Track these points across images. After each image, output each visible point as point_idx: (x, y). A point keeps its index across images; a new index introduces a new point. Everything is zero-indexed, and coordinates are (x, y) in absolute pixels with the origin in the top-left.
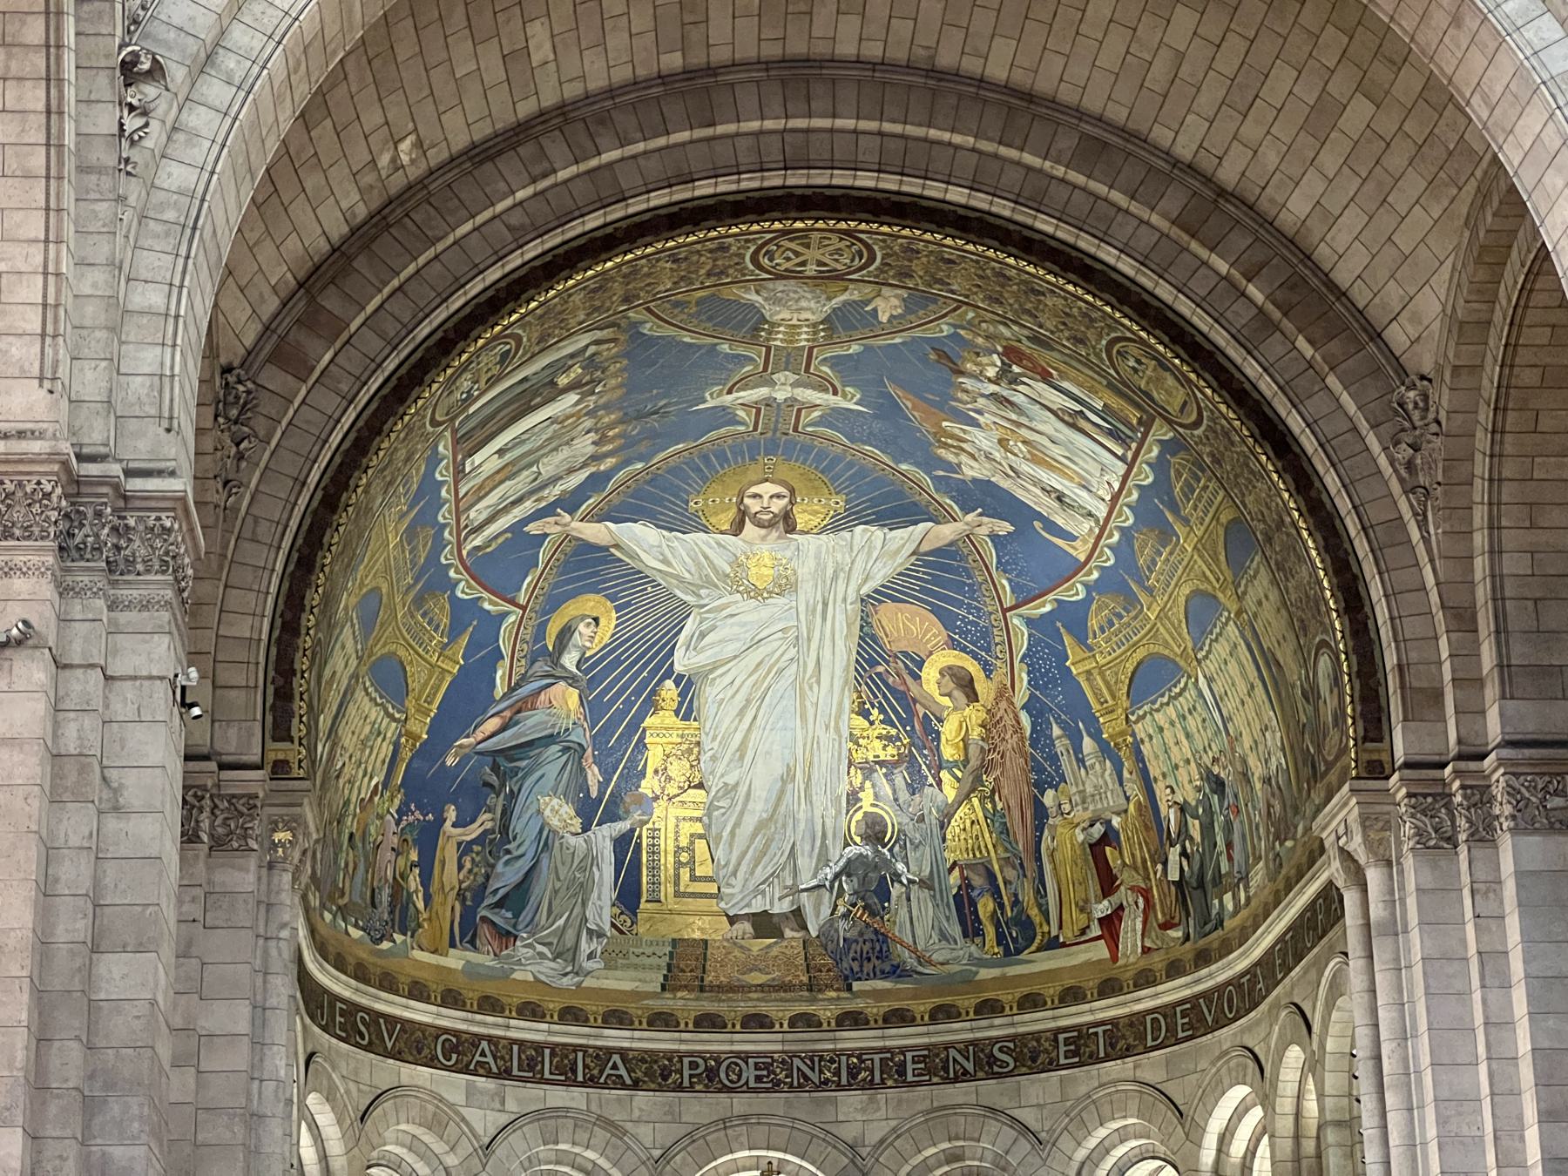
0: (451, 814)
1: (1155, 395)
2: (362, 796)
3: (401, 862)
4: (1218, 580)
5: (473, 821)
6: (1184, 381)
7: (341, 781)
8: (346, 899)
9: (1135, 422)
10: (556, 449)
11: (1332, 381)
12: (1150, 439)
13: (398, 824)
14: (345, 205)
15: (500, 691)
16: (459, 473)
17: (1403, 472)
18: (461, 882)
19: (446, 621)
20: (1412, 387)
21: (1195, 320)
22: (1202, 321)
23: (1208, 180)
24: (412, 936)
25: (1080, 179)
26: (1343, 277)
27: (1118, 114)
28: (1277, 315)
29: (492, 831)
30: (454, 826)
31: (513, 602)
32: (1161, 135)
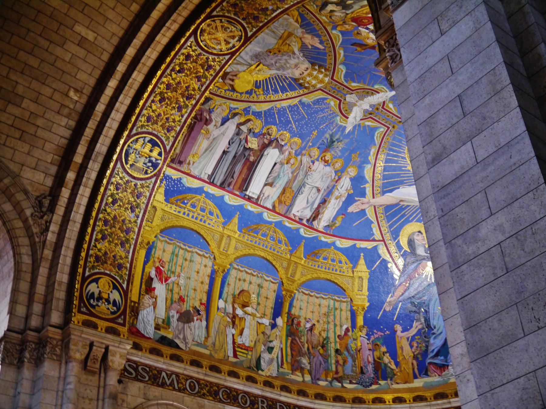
0: (398, 328)
2: (338, 333)
3: (377, 354)
5: (411, 327)
7: (316, 332)
8: (341, 374)
10: (306, 175)
13: (368, 339)
14: (63, 124)
15: (397, 274)
16: (249, 199)
18: (413, 353)
19: (344, 258)
24: (391, 380)
29: (423, 328)
30: (402, 332)
31: (374, 240)
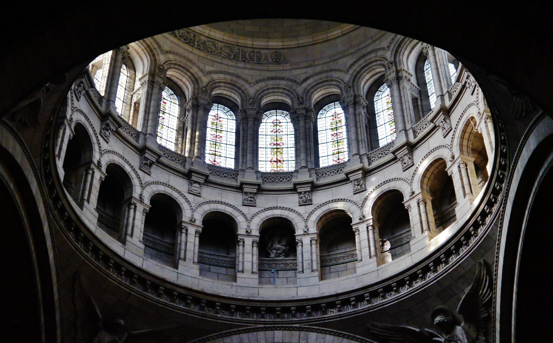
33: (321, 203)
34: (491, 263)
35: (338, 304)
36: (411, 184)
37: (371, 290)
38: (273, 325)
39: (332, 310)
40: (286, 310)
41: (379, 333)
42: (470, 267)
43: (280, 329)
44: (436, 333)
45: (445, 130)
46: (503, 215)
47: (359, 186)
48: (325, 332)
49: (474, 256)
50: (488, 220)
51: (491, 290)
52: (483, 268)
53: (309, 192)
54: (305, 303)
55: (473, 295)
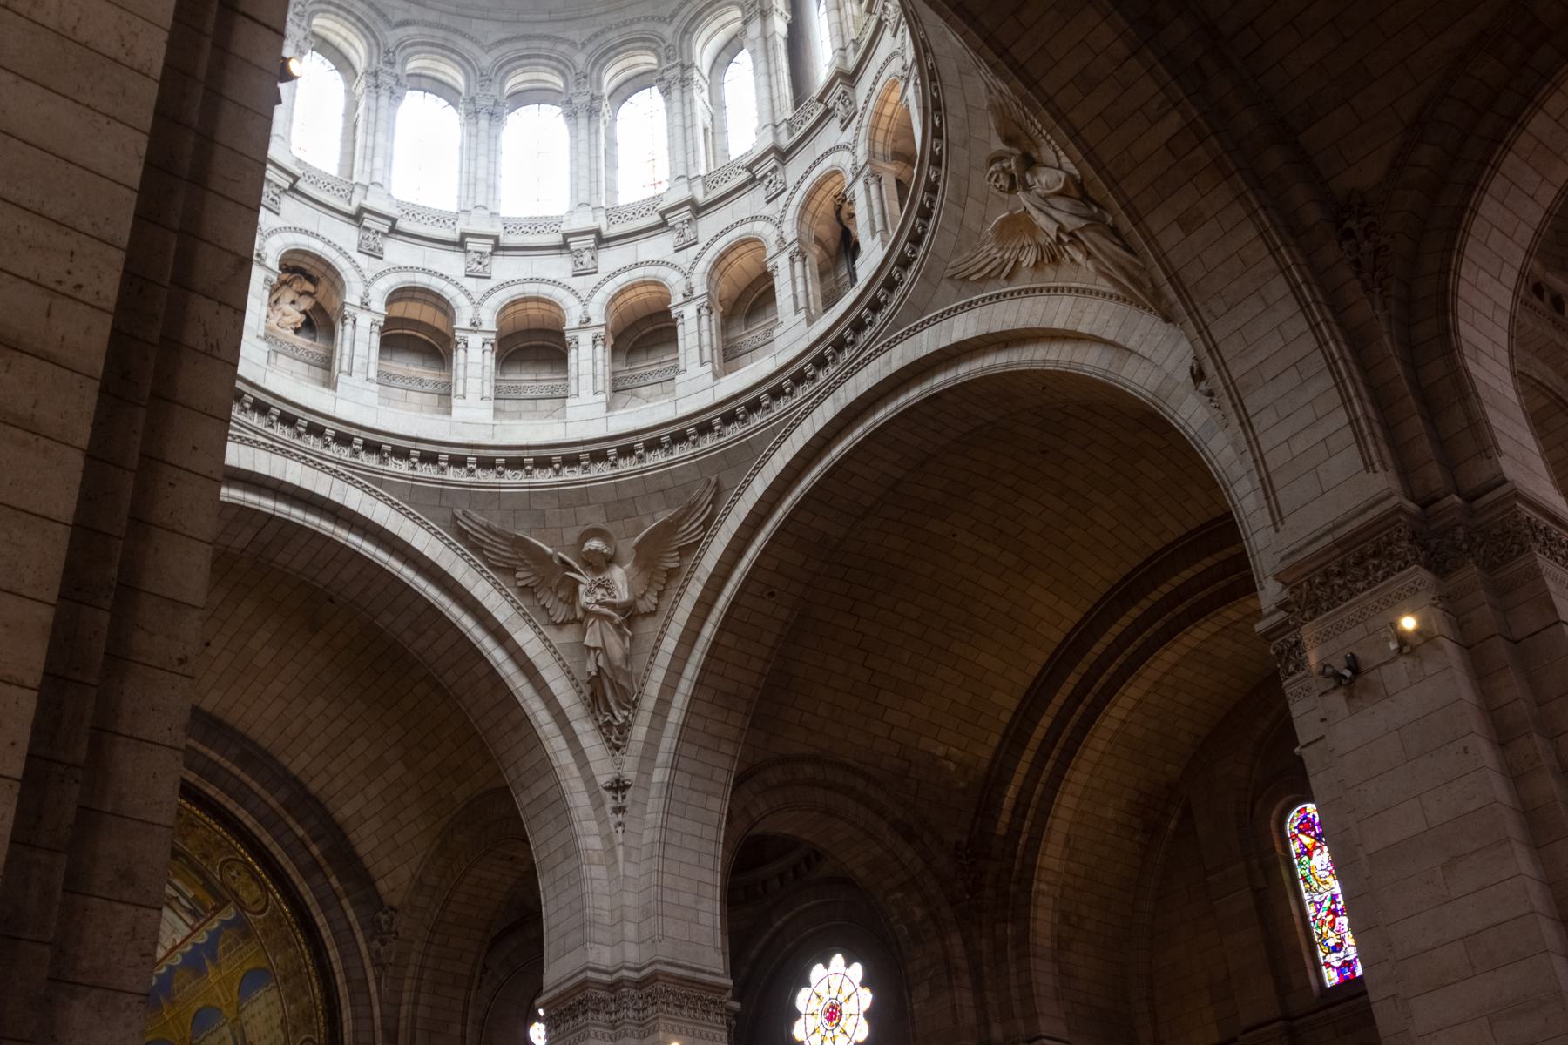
1: (241, 893)
4: (226, 1001)
6: (263, 887)
9: (210, 907)
11: (345, 902)
12: (216, 918)
17: (374, 955)
20: (386, 913)
21: (279, 858)
22: (282, 858)
23: (303, 787)
25: (236, 770)
26: (361, 850)
27: (264, 743)
28: (323, 862)
32: (285, 760)
33: (403, 264)
34: (727, 487)
35: (415, 457)
36: (585, 303)
37: (482, 453)
38: (287, 448)
39: (398, 462)
40: (316, 431)
41: (471, 531)
42: (686, 480)
43: (300, 459)
44: (577, 566)
45: (682, 240)
46: (800, 420)
47: (480, 267)
48: (378, 496)
49: (702, 464)
50: (758, 419)
51: (706, 530)
52: (709, 490)
53: (383, 234)
54: (354, 432)
55: (670, 527)
